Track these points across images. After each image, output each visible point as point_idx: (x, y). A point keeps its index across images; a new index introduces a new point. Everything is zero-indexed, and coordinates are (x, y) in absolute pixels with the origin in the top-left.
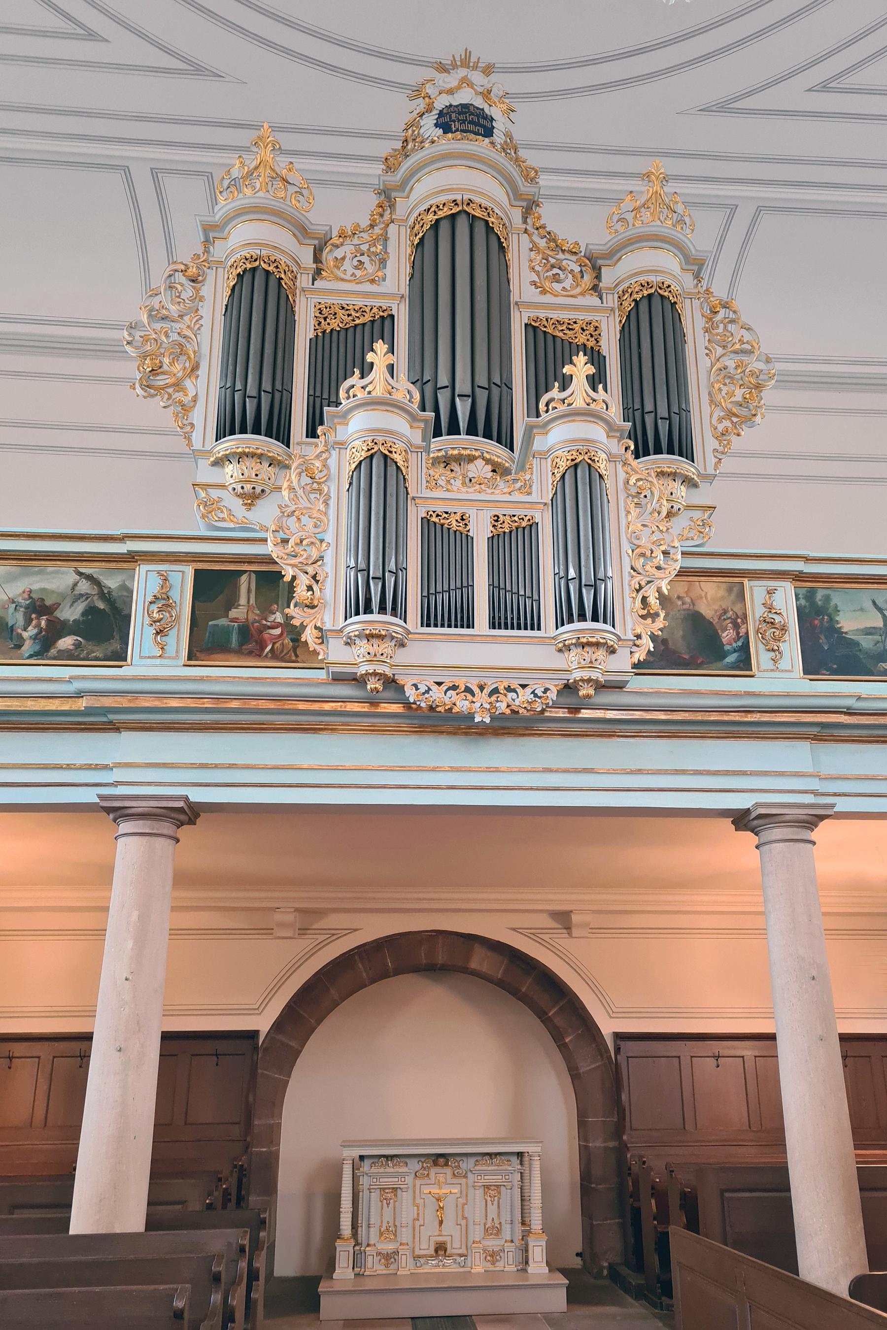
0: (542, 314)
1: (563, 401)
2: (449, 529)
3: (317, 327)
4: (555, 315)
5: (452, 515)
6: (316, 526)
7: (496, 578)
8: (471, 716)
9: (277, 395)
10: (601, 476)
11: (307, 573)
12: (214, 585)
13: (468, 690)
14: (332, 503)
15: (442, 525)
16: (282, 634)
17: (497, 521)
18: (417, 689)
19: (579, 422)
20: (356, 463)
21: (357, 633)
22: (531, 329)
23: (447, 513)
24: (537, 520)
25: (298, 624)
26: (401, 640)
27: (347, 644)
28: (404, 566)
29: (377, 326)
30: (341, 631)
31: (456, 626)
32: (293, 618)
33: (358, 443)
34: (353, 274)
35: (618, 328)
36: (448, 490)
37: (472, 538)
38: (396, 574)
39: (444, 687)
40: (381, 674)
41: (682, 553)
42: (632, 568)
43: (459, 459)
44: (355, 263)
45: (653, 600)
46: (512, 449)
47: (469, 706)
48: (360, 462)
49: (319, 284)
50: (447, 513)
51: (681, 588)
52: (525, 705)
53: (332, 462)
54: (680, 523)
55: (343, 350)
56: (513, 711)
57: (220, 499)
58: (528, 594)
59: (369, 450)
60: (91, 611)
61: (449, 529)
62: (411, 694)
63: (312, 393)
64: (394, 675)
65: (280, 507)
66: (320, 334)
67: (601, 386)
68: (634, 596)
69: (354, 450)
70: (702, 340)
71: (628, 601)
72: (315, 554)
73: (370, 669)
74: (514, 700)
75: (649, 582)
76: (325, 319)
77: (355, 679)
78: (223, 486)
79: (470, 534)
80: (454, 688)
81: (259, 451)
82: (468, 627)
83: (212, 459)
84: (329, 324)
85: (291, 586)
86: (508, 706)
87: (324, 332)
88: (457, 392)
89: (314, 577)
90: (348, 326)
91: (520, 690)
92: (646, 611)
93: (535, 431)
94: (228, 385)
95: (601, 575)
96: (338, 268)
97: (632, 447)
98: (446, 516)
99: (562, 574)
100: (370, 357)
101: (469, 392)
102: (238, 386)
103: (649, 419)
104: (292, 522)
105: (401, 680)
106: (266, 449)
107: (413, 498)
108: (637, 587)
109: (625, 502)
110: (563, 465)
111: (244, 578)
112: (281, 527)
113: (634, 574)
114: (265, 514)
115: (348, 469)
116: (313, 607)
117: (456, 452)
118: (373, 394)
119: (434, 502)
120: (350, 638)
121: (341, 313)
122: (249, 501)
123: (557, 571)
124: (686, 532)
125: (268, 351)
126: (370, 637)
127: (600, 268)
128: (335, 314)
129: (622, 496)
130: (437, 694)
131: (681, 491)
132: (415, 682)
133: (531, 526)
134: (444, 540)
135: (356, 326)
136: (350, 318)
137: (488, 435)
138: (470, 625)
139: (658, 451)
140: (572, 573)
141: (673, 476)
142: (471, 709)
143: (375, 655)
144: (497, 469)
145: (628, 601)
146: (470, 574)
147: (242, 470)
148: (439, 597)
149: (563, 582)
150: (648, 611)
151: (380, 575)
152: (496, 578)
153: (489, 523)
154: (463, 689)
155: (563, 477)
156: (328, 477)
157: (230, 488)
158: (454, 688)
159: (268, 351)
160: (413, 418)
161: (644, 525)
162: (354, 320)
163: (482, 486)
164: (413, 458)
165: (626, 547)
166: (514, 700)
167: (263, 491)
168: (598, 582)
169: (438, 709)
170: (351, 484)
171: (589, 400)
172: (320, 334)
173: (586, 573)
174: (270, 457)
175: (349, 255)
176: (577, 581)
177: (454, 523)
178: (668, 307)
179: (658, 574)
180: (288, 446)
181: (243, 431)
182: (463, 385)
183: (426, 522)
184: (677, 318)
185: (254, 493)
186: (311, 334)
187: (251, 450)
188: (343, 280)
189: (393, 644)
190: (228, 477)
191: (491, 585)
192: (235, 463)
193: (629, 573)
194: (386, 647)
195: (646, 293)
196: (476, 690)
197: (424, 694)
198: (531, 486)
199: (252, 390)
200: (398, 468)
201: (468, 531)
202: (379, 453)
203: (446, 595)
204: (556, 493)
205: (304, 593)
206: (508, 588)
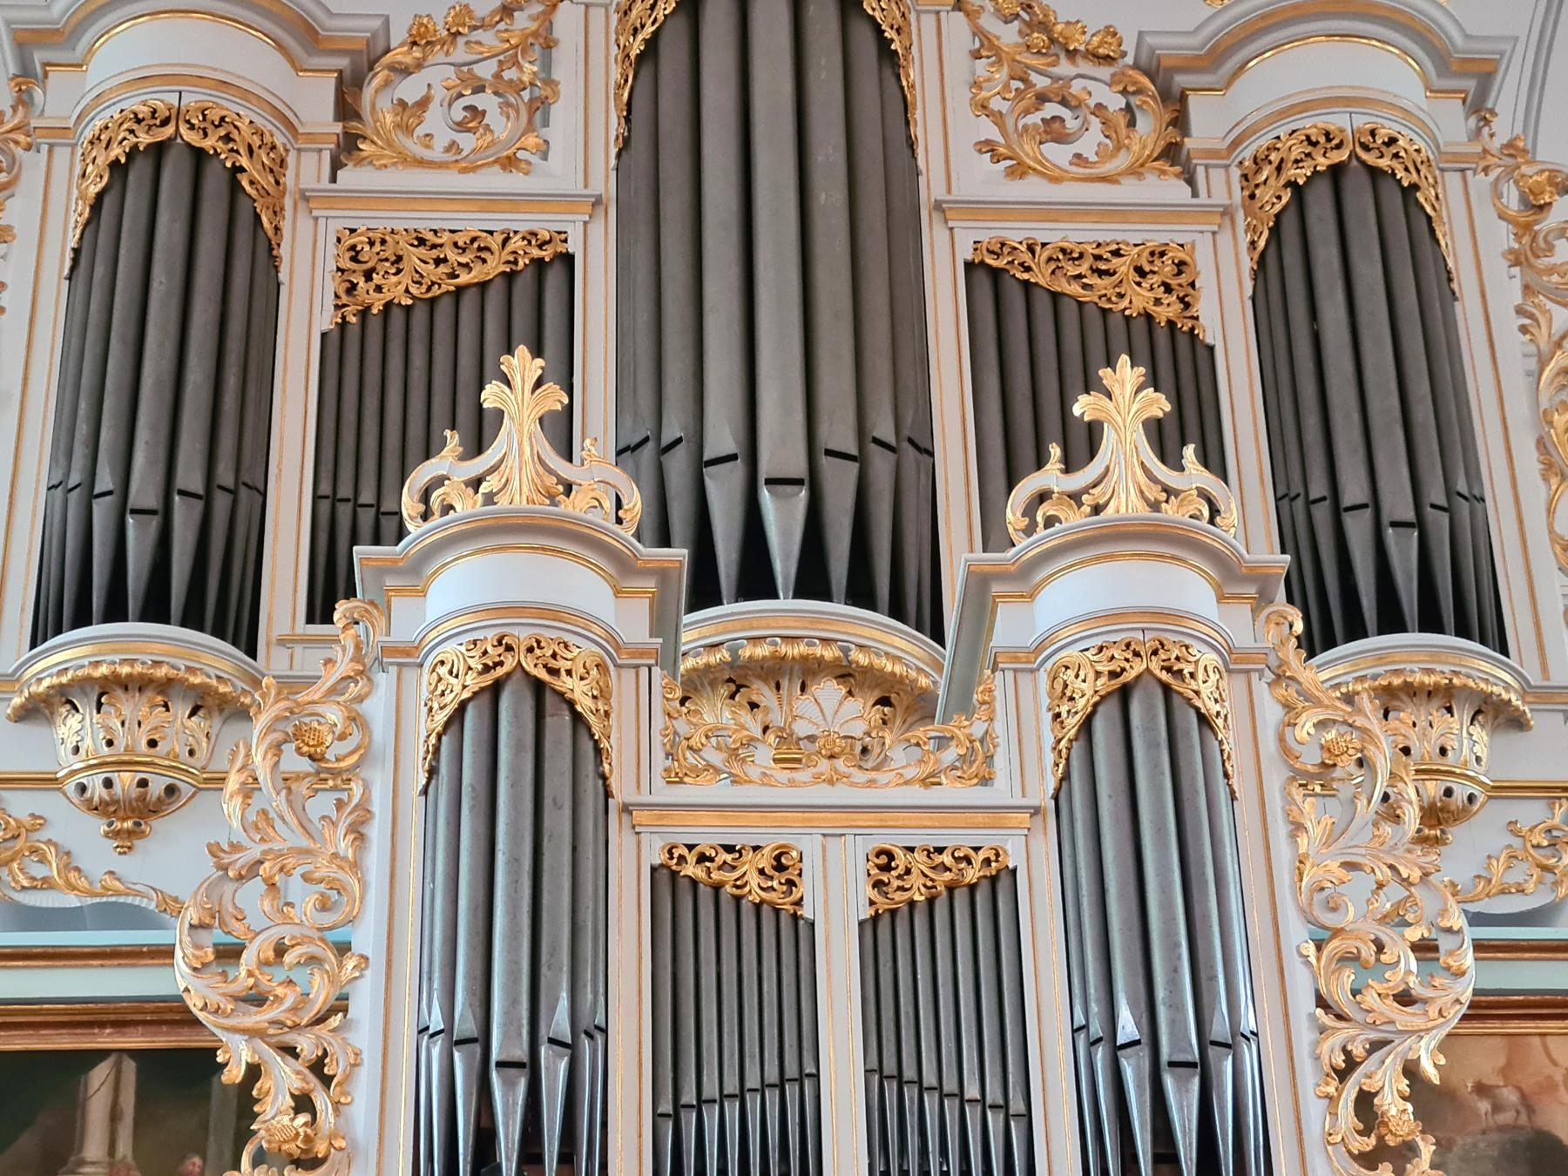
0: (1016, 233)
1: (1075, 497)
3: (345, 299)
4: (1054, 234)
6: (324, 906)
9: (221, 502)
10: (1203, 720)
11: (296, 1056)
14: (377, 831)
15: (717, 888)
17: (886, 868)
19: (1124, 561)
22: (987, 278)
23: (729, 849)
24: (1014, 857)
28: (600, 1020)
29: (523, 288)
33: (450, 650)
34: (453, 146)
35: (1247, 264)
36: (736, 780)
38: (572, 1048)
41: (1480, 947)
42: (1321, 1002)
43: (774, 672)
44: (458, 113)
45: (1394, 1106)
46: (938, 635)
49: (350, 177)
50: (729, 849)
51: (1485, 1060)
54: (1472, 849)
55: (417, 365)
57: (39, 822)
58: (994, 1094)
61: (738, 900)
65: (214, 850)
67: (1189, 452)
68: (1331, 1090)
70: (1507, 289)
71: (1314, 1109)
72: (321, 995)
75: (1376, 1046)
76: (368, 276)
78: (49, 782)
79: (806, 912)
81: (161, 672)
83: (18, 700)
84: (379, 289)
85: (245, 1099)
87: (364, 313)
89: (317, 1067)
90: (436, 291)
92: (1373, 1141)
93: (996, 588)
94: (74, 479)
95: (1219, 1028)
96: (409, 131)
97: (1299, 627)
98: (729, 858)
99: (1096, 1029)
100: (492, 395)
102: (105, 481)
103: (1358, 529)
104: (251, 896)
106: (181, 664)
107: (626, 809)
108: (1340, 1060)
109: (1288, 799)
110: (1086, 690)
111: (100, 1075)
113: (1328, 1020)
114: (172, 862)
115: (423, 726)
116: (313, 1163)
117: (762, 651)
118: (503, 502)
121: (413, 256)
122: (128, 824)
123: (1080, 1019)
124: (1498, 868)
127: (1183, 98)
128: (399, 259)
129: (1275, 779)
131: (1472, 742)
133: (994, 880)
135: (460, 290)
136: (443, 269)
139: (1392, 622)
140: (1128, 1026)
141: (1445, 696)
144: (894, 697)
145: (1314, 1109)
146: (809, 1041)
147: (108, 729)
149: (1100, 1053)
150: (1381, 1138)
151: (521, 1053)
155: (1087, 726)
156: (365, 752)
157: (70, 787)
160: (623, 566)
161: (1350, 866)
162: (453, 276)
163: (840, 763)
164: (623, 686)
165: (1297, 935)
167: (171, 790)
168: (1212, 1052)
170: (432, 772)
171: (1154, 493)
172: (353, 320)
173: (1172, 1023)
174: (193, 687)
175: (439, 94)
176: (1144, 1052)
177: (754, 880)
178: (1393, 202)
179: (1406, 1018)
180: (252, 652)
181: (115, 612)
183: (666, 880)
184: (1422, 229)
186: (326, 320)
187: (138, 669)
188: (421, 163)
190: (64, 752)
191: (875, 1072)
192: (86, 708)
193: (1312, 1017)
195: (1322, 163)
198: (989, 759)
199: (144, 491)
201: (799, 903)
203: (732, 1110)
204: (1066, 777)
205: (286, 1120)
206: (929, 1078)
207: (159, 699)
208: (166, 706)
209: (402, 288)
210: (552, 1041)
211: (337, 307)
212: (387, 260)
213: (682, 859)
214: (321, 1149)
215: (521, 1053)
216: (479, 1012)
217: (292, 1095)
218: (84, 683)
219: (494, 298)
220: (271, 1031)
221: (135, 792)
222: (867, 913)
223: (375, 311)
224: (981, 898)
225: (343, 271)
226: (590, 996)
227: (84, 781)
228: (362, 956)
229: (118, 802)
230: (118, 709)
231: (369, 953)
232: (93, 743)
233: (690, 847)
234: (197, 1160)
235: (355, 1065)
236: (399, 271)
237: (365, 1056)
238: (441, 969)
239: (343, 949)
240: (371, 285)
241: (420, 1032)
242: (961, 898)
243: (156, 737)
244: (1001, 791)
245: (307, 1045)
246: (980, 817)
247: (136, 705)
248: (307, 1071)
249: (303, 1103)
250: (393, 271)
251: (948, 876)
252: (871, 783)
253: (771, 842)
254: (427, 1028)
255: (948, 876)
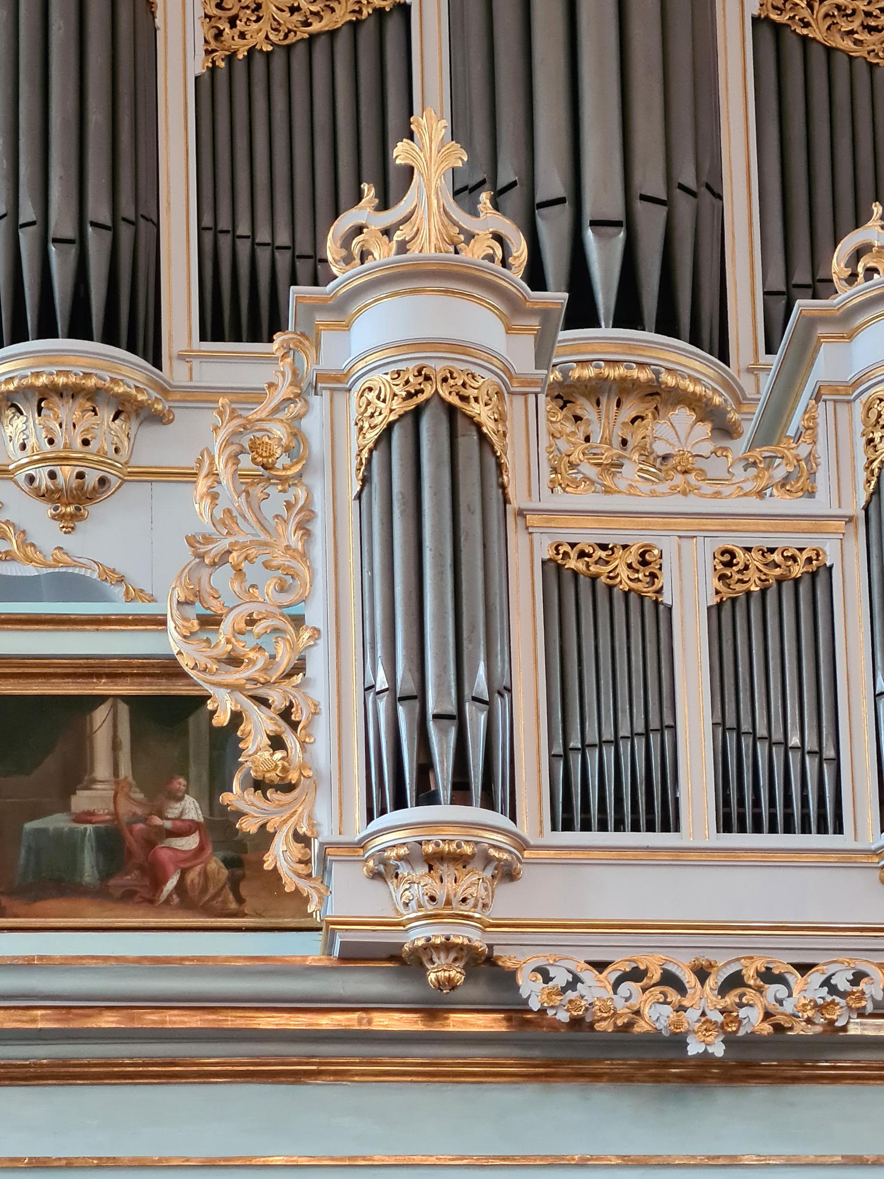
2: (610, 588)
5: (619, 552)
6: (282, 589)
7: (730, 707)
8: (678, 1041)
13: (670, 980)
14: (320, 528)
15: (594, 579)
16: (201, 849)
17: (729, 564)
18: (547, 979)
20: (378, 431)
21: (403, 851)
23: (604, 547)
25: (253, 829)
26: (508, 864)
27: (376, 875)
29: (367, 35)
30: (361, 845)
31: (635, 828)
32: (245, 814)
36: (608, 491)
37: (670, 609)
39: (611, 974)
40: (461, 947)
47: (673, 1016)
48: (390, 426)
50: (604, 547)
52: (810, 1013)
53: (314, 425)
56: (778, 1028)
59: (410, 396)
61: (610, 588)
62: (532, 990)
63: (208, 221)
64: (490, 947)
66: (222, 64)
69: (371, 396)
72: (285, 659)
73: (437, 933)
74: (780, 1002)
77: (392, 958)
79: (666, 599)
80: (636, 975)
82: (665, 828)
84: (242, 35)
86: (767, 1015)
88: (588, 213)
89: (286, 714)
90: (292, 39)
91: (794, 978)
98: (603, 554)
101: (617, 212)
105: (508, 958)
107: (521, 513)
112: (198, 594)
115: (355, 444)
116: (289, 788)
119: (572, 520)
120: (384, 862)
122: (70, 509)
125: (97, 116)
126: (433, 861)
128: (259, 7)
130: (595, 990)
132: (541, 962)
133: (814, 575)
134: (601, 612)
135: (313, 37)
136: (297, 17)
137: (667, 325)
138: (670, 822)
142: (678, 1024)
143: (448, 903)
146: (667, 698)
147: (49, 430)
148: (593, 758)
151: (451, 708)
152: (730, 707)
153: (710, 569)
154: (657, 977)
157: (21, 476)
158: (636, 975)
159: (97, 116)
162: (307, 24)
166: (780, 1002)
167: (103, 481)
169: (600, 1026)
170: (366, 481)
177: (624, 573)
182: (602, 196)
183: (554, 571)
185: (81, 488)
186: (198, 65)
189: (488, 873)
190: (13, 448)
192: (30, 412)
194: (472, 883)
196: (689, 979)
197: (564, 990)
200: (483, 438)
201: (659, 591)
202: (435, 402)
205: (267, 755)
207: (88, 405)
208: (94, 410)
209: (262, 35)
210: (475, 699)
211: (208, 52)
212: (247, 7)
213: (566, 555)
214: (293, 777)
215: (451, 708)
216: (417, 675)
217: (268, 736)
218: (25, 391)
219: (342, 45)
220: (248, 686)
221: (75, 483)
222: (714, 600)
223: (240, 57)
224: (803, 589)
225: (210, 17)
226: (499, 664)
227: (32, 472)
228: (315, 629)
229: (61, 490)
230: (55, 413)
231: (320, 626)
232: (37, 440)
233: (573, 545)
234: (182, 780)
235: (315, 714)
236: (259, 19)
237: (323, 707)
238: (383, 640)
239: (298, 621)
240: (236, 31)
241: (366, 690)
242: (787, 588)
243: (88, 437)
244: (820, 504)
245: (276, 697)
246: (805, 524)
247: (70, 410)
248: (278, 718)
249: (277, 743)
250: (254, 18)
251: (778, 571)
252: (717, 495)
253: (637, 542)
254: (373, 687)
255: (778, 571)
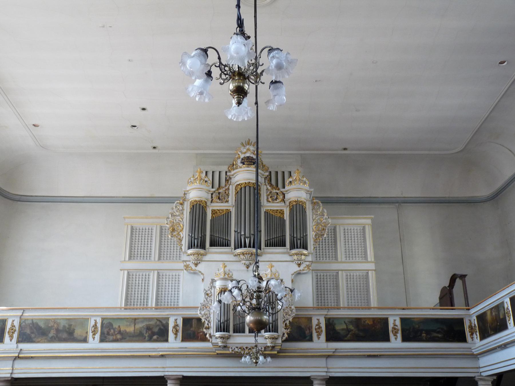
12: (187, 321)
60: (160, 329)
111: (194, 320)
